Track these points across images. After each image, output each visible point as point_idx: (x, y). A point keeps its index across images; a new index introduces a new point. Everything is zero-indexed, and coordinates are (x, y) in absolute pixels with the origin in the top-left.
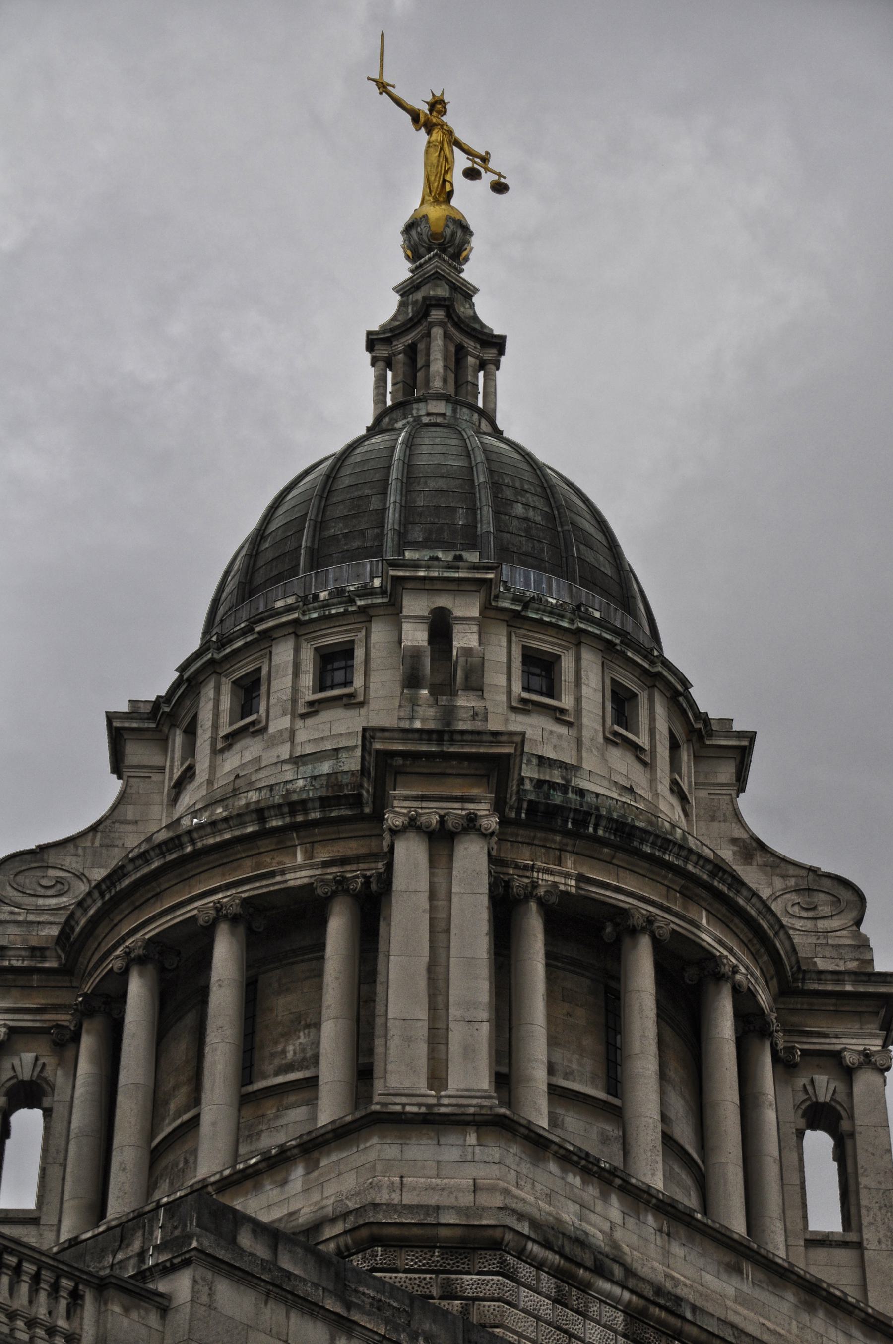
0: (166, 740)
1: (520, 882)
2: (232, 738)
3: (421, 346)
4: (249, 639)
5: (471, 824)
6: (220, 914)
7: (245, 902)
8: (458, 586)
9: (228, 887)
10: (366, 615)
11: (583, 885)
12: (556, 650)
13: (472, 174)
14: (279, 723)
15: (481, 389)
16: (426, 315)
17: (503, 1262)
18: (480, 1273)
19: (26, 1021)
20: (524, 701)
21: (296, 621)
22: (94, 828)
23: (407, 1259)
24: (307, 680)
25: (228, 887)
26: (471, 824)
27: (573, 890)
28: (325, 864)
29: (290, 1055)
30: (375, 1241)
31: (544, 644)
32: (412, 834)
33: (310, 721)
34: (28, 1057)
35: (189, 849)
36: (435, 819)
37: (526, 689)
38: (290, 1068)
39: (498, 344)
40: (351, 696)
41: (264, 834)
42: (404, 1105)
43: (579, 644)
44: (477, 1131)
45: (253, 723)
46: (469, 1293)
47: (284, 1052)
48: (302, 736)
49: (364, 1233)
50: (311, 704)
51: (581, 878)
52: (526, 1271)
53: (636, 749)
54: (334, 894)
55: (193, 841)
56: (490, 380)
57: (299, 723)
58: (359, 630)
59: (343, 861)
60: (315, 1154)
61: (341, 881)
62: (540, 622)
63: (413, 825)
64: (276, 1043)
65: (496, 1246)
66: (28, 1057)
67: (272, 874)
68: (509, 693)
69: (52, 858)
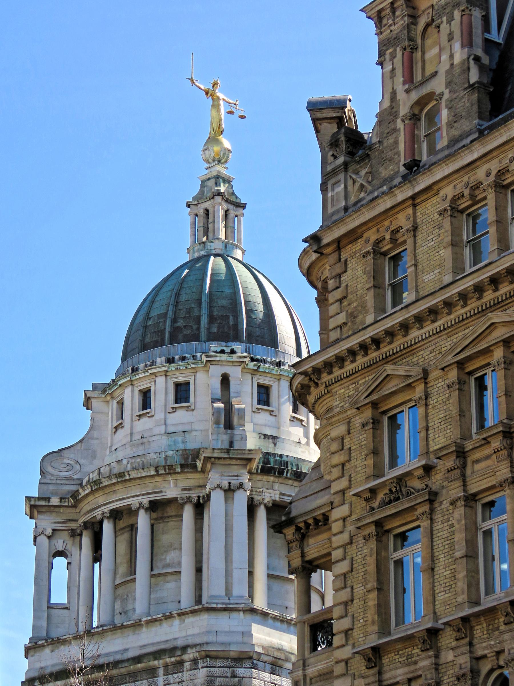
0: (108, 402)
1: (257, 498)
2: (140, 416)
3: (211, 212)
4: (146, 374)
5: (241, 486)
6: (141, 506)
7: (151, 502)
8: (233, 363)
9: (144, 495)
10: (195, 370)
11: (282, 497)
12: (270, 383)
13: (231, 113)
14: (160, 415)
15: (236, 229)
16: (213, 198)
17: (253, 663)
18: (245, 668)
19: (59, 526)
20: (258, 409)
21: (166, 371)
22: (81, 441)
23: (218, 663)
24: (171, 396)
25: (144, 495)
26: (241, 486)
27: (277, 499)
28: (183, 490)
29: (168, 560)
30: (207, 656)
31: (265, 381)
32: (218, 490)
33: (172, 415)
34: (61, 541)
35: (127, 477)
36: (227, 485)
37: (259, 403)
38: (168, 566)
39: (243, 206)
40: (188, 407)
41: (158, 475)
42: (217, 604)
43: (279, 380)
44: (244, 613)
45: (148, 413)
46: (241, 676)
47: (165, 559)
48: (169, 422)
49: (203, 653)
50: (173, 408)
51: (281, 494)
52: (261, 664)
53: (302, 421)
54: (186, 502)
55: (129, 475)
56: (239, 222)
57: (168, 415)
58: (192, 376)
59: (189, 489)
60: (183, 617)
61: (189, 498)
62: (265, 372)
63: (218, 486)
64: (162, 554)
65: (251, 658)
66: (61, 541)
67: (161, 492)
68: (252, 405)
69: (65, 453)
